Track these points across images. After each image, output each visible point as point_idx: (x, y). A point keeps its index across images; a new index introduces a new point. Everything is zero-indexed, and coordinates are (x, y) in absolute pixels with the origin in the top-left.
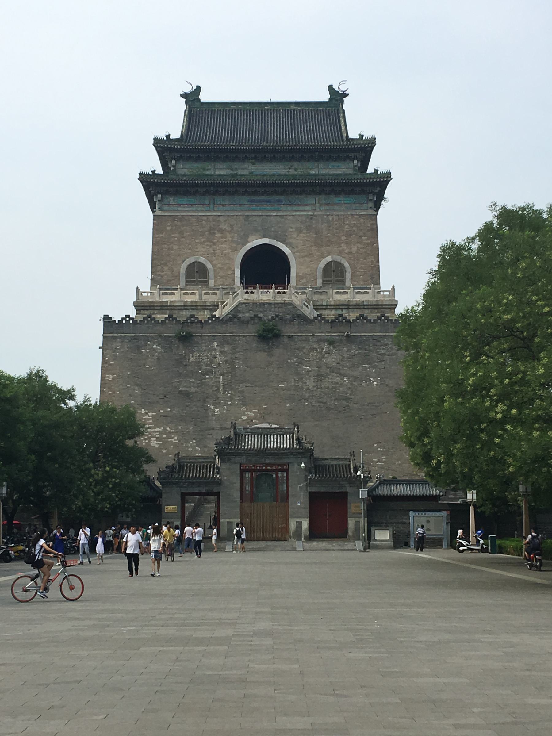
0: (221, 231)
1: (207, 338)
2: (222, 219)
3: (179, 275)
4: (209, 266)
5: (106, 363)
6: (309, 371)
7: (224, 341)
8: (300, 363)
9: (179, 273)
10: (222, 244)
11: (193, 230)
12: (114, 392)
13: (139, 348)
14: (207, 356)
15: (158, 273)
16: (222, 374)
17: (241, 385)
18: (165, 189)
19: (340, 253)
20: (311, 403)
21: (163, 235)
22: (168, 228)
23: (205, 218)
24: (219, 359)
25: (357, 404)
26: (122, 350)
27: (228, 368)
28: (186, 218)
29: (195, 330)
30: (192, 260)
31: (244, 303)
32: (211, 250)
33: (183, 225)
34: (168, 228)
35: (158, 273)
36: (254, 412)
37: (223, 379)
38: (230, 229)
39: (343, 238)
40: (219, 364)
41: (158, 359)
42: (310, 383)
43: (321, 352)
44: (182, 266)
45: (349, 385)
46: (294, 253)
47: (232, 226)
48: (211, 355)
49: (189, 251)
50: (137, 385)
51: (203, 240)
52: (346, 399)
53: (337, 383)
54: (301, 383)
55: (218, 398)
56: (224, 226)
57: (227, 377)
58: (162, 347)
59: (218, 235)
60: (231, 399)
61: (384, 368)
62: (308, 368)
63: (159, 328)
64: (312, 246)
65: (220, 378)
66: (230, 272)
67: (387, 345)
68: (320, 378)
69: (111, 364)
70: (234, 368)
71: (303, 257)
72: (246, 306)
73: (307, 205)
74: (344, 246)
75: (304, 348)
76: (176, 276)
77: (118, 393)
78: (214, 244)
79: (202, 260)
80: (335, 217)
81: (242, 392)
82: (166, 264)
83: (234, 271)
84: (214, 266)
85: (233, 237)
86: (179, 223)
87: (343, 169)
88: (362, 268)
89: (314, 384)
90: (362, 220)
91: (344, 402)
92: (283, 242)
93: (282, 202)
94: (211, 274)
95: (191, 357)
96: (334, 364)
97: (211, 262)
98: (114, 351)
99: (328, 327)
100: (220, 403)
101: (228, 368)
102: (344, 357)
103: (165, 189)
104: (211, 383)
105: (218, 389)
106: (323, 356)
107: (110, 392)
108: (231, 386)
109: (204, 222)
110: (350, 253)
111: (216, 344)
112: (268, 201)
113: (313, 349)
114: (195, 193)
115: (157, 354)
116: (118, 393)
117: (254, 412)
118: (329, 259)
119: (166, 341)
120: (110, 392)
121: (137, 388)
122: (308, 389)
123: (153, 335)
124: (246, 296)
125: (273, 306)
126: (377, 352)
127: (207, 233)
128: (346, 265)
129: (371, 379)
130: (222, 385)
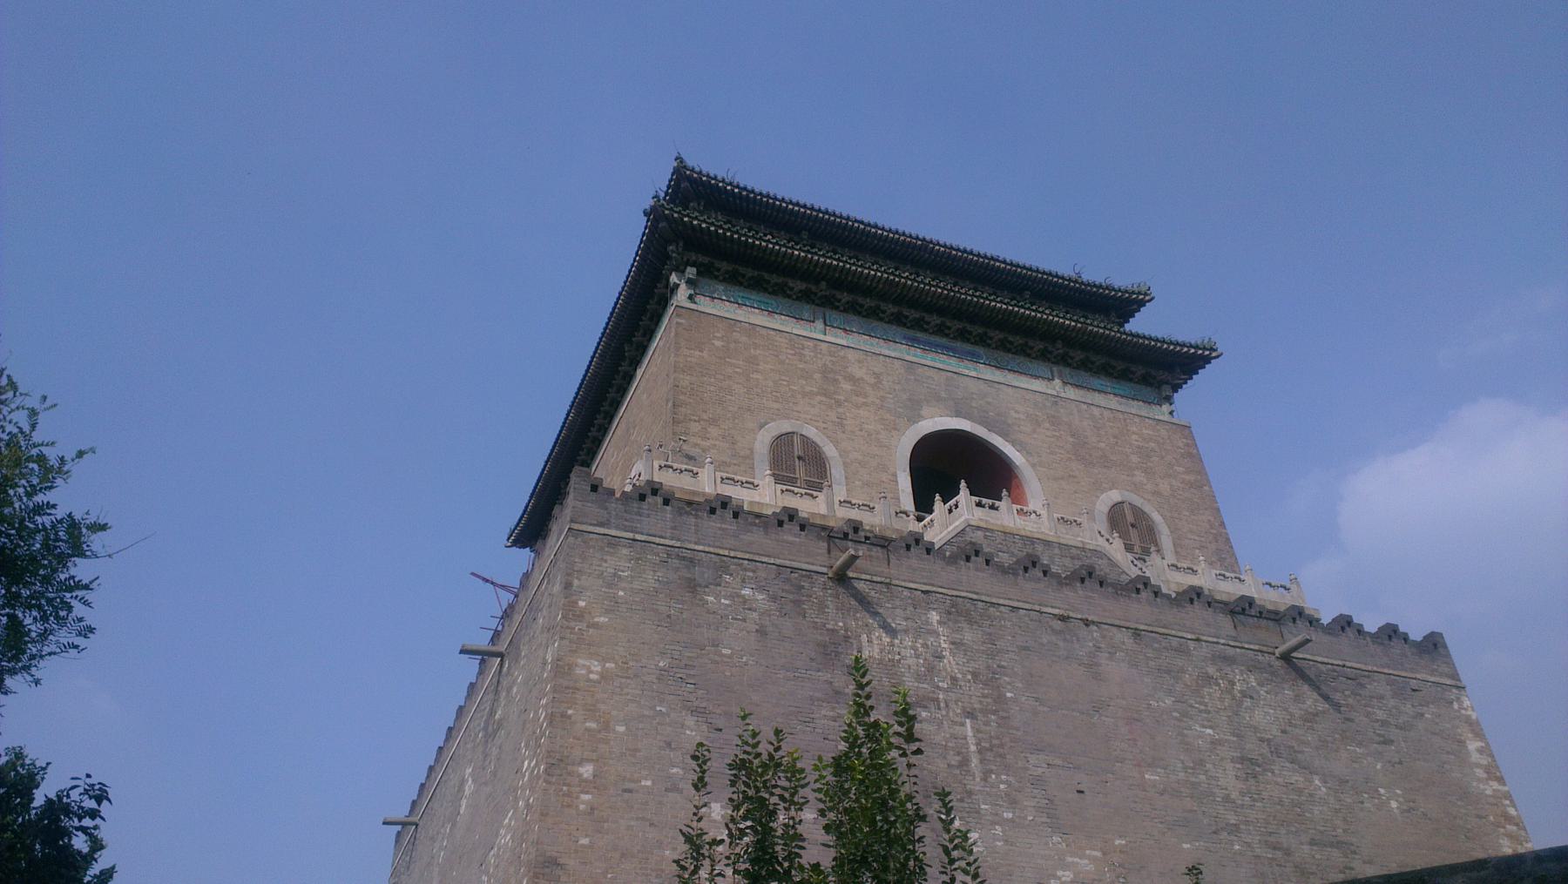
0: (851, 379)
1: (906, 593)
2: (851, 355)
3: (750, 456)
4: (829, 450)
5: (580, 616)
6: (1215, 743)
7: (956, 611)
8: (1185, 714)
9: (751, 450)
10: (858, 407)
11: (782, 362)
12: (606, 727)
13: (692, 587)
14: (914, 648)
15: (693, 440)
16: (970, 714)
17: (1033, 759)
18: (706, 260)
19: (1137, 488)
20: (1249, 845)
21: (705, 354)
22: (718, 343)
23: (811, 344)
24: (950, 663)
25: (1370, 862)
26: (636, 585)
27: (984, 696)
28: (764, 332)
29: (869, 567)
30: (786, 426)
31: (979, 528)
32: (833, 416)
33: (756, 346)
34: (718, 343)
35: (693, 440)
36: (1093, 859)
37: (977, 731)
38: (873, 381)
39: (1134, 459)
40: (954, 679)
41: (762, 632)
42: (1229, 779)
43: (1230, 691)
44: (759, 437)
45: (1332, 800)
46: (1033, 466)
47: (877, 376)
48: (925, 645)
49: (776, 406)
50: (694, 711)
51: (808, 389)
52: (1338, 844)
53: (1300, 792)
54: (1203, 777)
55: (970, 793)
56: (859, 373)
57: (987, 724)
58: (774, 598)
59: (847, 386)
60: (1013, 803)
61: (1400, 763)
62: (1209, 731)
63: (756, 537)
64: (1069, 459)
65: (963, 724)
66: (884, 477)
67: (1382, 697)
68: (1251, 767)
69: (596, 626)
70: (1000, 699)
71: (1056, 479)
72: (986, 537)
73: (1037, 377)
74: (1140, 477)
75: (1182, 671)
76: (745, 458)
77: (621, 729)
78: (839, 404)
79: (811, 432)
80: (1106, 413)
81: (1038, 782)
82: (714, 421)
83: (895, 475)
84: (843, 453)
85: (882, 399)
86: (744, 339)
87: (1097, 326)
88: (1191, 531)
89: (1240, 785)
90: (1163, 433)
91: (1336, 853)
92: (1004, 435)
93: (979, 356)
94: (836, 471)
95: (865, 644)
96: (1275, 732)
97: (836, 443)
98: (610, 586)
99: (1225, 622)
100: (978, 812)
101: (984, 696)
102: (1291, 715)
103: (706, 260)
104: (938, 739)
105: (965, 762)
106: (1240, 704)
107: (593, 725)
108: (1002, 756)
109: (806, 352)
110: (1157, 493)
111: (934, 617)
112: (948, 349)
113: (1208, 679)
114: (780, 291)
115: (755, 615)
116: (621, 729)
117: (1093, 859)
118: (1115, 496)
119: (792, 581)
120: (593, 725)
121: (690, 721)
122: (1227, 799)
123: (739, 555)
124: (979, 512)
125: (1057, 551)
126: (1368, 715)
127: (817, 376)
128: (1156, 517)
129: (1382, 791)
130: (973, 748)
